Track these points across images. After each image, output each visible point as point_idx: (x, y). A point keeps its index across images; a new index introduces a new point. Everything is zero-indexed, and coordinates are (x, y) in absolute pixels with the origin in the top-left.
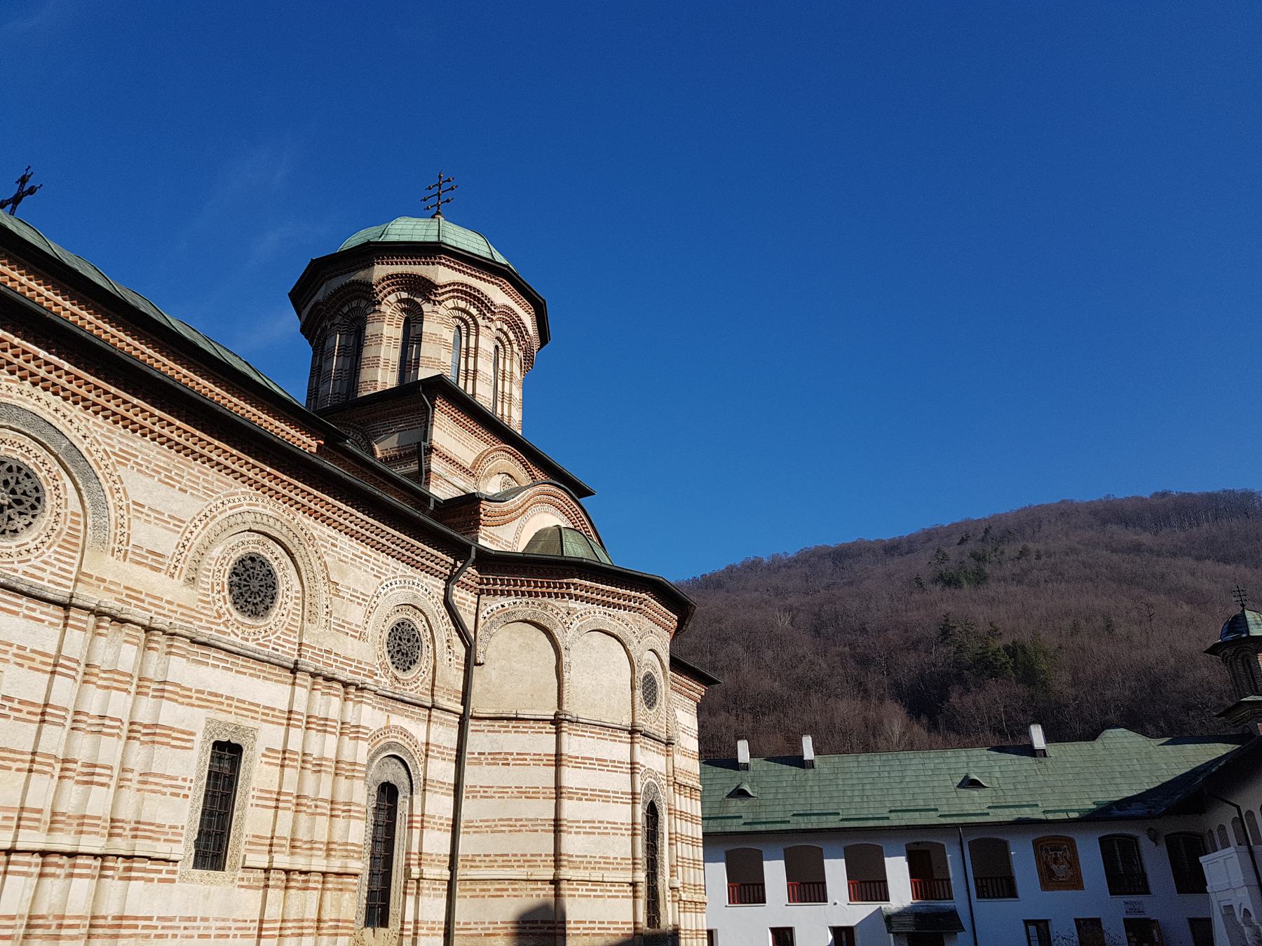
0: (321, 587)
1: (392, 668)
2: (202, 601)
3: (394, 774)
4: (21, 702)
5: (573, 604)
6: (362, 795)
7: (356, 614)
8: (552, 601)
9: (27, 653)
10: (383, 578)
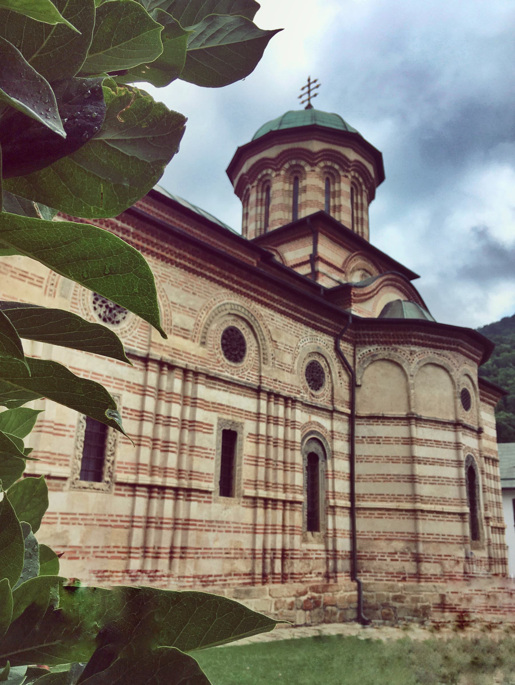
0: (269, 344)
1: (309, 389)
2: (209, 354)
3: (314, 448)
4: (132, 410)
5: (413, 348)
6: (299, 458)
7: (287, 359)
8: (401, 347)
9: (131, 385)
10: (300, 337)
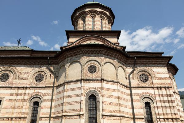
0: (17, 74)
7: (26, 76)
